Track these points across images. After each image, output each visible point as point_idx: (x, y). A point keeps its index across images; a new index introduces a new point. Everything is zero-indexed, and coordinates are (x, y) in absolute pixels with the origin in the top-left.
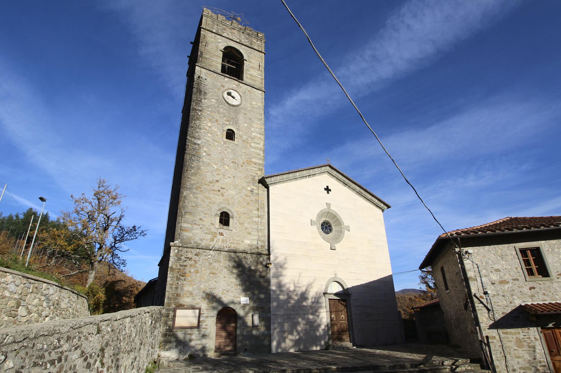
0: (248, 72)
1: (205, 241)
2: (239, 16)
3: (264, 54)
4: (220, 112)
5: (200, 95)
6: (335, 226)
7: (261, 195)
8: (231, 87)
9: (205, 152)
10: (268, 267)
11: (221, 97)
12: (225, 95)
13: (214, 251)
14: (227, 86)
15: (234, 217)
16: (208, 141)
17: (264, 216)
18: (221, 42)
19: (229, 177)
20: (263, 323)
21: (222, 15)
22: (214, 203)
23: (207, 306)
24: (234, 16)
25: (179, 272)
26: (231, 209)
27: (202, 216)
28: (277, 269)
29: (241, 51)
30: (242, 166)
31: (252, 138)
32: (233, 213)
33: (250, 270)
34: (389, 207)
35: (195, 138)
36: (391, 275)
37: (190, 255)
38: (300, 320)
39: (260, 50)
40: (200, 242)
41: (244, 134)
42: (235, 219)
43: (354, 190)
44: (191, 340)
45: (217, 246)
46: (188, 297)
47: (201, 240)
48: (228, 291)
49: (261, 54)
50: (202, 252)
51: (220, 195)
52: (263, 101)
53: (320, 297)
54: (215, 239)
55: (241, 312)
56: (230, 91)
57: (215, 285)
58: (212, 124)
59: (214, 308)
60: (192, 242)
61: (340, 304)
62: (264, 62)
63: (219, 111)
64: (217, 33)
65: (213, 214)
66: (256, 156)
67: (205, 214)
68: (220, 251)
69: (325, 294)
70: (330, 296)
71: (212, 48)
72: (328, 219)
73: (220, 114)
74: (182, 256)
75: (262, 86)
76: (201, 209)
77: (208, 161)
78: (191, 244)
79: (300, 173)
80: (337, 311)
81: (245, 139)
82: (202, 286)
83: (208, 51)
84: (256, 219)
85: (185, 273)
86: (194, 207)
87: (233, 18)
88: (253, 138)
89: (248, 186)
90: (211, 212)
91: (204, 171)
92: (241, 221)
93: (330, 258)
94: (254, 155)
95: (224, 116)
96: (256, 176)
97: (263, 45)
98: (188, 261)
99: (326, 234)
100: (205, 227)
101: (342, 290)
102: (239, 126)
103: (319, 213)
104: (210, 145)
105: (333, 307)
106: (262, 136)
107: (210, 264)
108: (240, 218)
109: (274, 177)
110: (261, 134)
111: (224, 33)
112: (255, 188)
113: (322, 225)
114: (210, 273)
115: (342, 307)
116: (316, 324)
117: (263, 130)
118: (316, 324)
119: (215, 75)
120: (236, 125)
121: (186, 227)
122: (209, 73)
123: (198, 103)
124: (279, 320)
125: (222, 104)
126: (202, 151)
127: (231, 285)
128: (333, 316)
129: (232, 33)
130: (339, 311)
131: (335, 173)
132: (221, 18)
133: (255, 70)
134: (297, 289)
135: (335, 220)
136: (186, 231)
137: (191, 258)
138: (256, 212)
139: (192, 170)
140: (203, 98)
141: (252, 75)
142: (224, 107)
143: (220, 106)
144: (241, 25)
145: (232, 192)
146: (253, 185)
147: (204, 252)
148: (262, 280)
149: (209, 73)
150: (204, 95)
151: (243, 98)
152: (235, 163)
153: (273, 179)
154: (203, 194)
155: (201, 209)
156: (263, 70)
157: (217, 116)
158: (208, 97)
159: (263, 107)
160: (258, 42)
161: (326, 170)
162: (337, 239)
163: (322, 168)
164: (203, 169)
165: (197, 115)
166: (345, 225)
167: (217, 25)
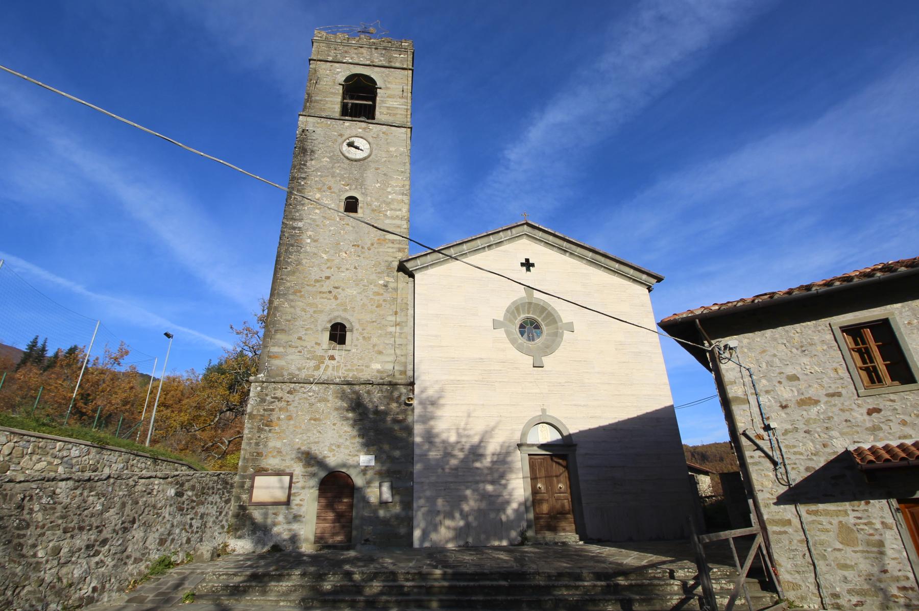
1: (305, 370)
5: (304, 156)
6: (546, 325)
7: (402, 289)
9: (310, 237)
10: (411, 405)
11: (337, 152)
12: (345, 148)
13: (318, 385)
14: (347, 133)
15: (354, 329)
16: (314, 220)
18: (341, 72)
19: (347, 269)
20: (397, 498)
22: (321, 312)
23: (303, 470)
24: (365, 28)
25: (262, 419)
26: (349, 317)
27: (302, 333)
28: (425, 408)
29: (372, 76)
30: (369, 249)
31: (388, 204)
32: (353, 323)
33: (377, 412)
34: (659, 280)
35: (295, 220)
36: (672, 406)
37: (279, 394)
38: (468, 492)
39: (405, 66)
40: (297, 372)
42: (355, 332)
43: (581, 258)
44: (274, 524)
45: (324, 377)
46: (274, 457)
47: (299, 369)
48: (339, 446)
49: (406, 72)
50: (298, 388)
51: (332, 298)
52: (409, 141)
53: (508, 454)
54: (323, 366)
55: (359, 481)
56: (352, 139)
57: (319, 437)
58: (321, 195)
59: (313, 475)
60: (285, 373)
61: (554, 464)
63: (334, 172)
65: (320, 328)
67: (306, 330)
68: (328, 384)
70: (531, 448)
72: (532, 314)
73: (336, 177)
74: (267, 395)
75: (408, 121)
76: (301, 323)
77: (314, 250)
78: (283, 376)
79: (469, 244)
80: (549, 477)
82: (297, 440)
84: (392, 329)
85: (271, 421)
86: (289, 321)
88: (390, 203)
89: (380, 278)
90: (316, 326)
91: (307, 265)
92: (366, 335)
93: (531, 382)
95: (343, 178)
96: (393, 261)
101: (559, 437)
103: (510, 307)
104: (317, 226)
107: (311, 405)
108: (363, 330)
109: (421, 258)
110: (403, 194)
111: (346, 57)
112: (391, 280)
113: (522, 326)
114: (310, 419)
115: (557, 469)
116: (500, 500)
117: (407, 187)
118: (500, 500)
120: (361, 188)
122: (319, 121)
123: (301, 168)
124: (428, 493)
126: (304, 236)
127: (345, 437)
128: (539, 485)
129: (359, 53)
130: (554, 476)
133: (395, 99)
134: (464, 440)
135: (544, 314)
138: (393, 318)
141: (389, 107)
142: (342, 165)
143: (336, 165)
145: (352, 291)
146: (388, 276)
147: (302, 387)
148: (396, 427)
149: (319, 121)
150: (311, 155)
152: (358, 246)
153: (419, 262)
154: (304, 301)
155: (301, 323)
157: (330, 181)
158: (316, 156)
159: (409, 152)
160: (401, 56)
161: (523, 232)
162: (547, 347)
164: (306, 263)
165: (299, 185)
167: (336, 49)
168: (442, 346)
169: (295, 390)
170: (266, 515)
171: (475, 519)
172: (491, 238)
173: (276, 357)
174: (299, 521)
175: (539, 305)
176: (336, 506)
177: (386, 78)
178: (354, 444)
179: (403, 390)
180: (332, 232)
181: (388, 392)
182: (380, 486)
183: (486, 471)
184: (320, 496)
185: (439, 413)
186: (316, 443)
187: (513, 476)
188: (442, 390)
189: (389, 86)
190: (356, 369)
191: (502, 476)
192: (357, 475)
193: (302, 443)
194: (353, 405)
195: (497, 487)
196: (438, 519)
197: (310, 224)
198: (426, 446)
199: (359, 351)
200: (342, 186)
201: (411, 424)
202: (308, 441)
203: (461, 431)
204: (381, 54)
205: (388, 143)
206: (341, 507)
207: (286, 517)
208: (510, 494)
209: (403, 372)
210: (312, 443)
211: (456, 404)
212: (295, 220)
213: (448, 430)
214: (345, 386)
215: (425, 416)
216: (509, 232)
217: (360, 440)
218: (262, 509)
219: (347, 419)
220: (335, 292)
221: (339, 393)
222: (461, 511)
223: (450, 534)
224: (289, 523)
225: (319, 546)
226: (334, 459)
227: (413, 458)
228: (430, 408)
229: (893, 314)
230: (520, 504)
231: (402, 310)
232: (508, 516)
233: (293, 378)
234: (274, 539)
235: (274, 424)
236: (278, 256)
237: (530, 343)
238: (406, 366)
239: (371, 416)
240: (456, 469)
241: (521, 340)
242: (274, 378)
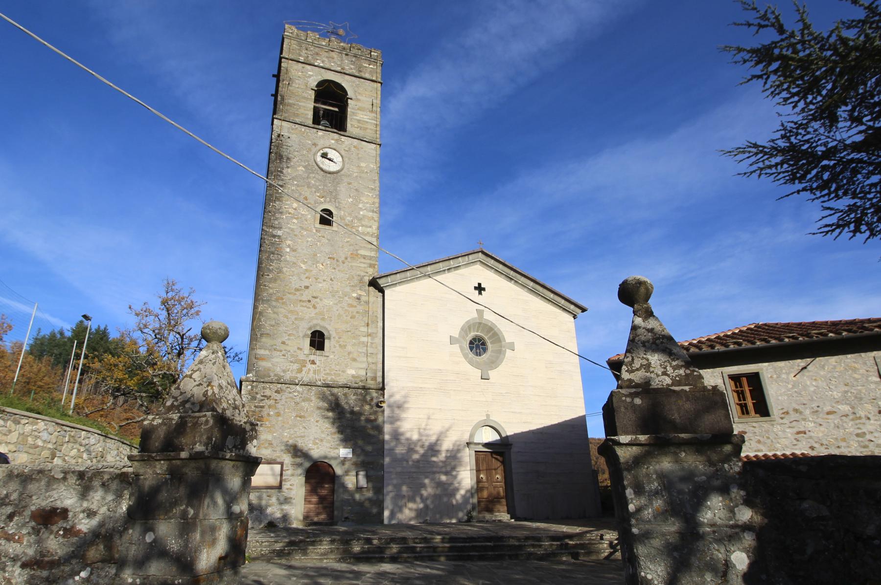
0: (355, 117)
3: (380, 84)
4: (311, 185)
5: (280, 163)
7: (373, 303)
8: (327, 144)
9: (289, 246)
10: (382, 407)
11: (312, 163)
12: (319, 159)
13: (302, 386)
14: (321, 143)
15: (332, 337)
16: (292, 230)
17: (376, 333)
18: (312, 75)
19: (324, 281)
20: (370, 485)
21: (313, 30)
22: (302, 319)
23: (292, 460)
24: (334, 28)
26: (327, 326)
28: (393, 411)
29: (343, 85)
30: (343, 263)
31: (360, 220)
33: (352, 412)
35: (274, 227)
37: (268, 393)
39: (374, 78)
40: (282, 374)
41: (347, 214)
42: (332, 340)
45: (306, 380)
47: (284, 371)
48: (322, 440)
49: (375, 85)
50: (285, 388)
52: (378, 159)
55: (339, 471)
56: (326, 150)
58: (298, 205)
60: (272, 374)
62: (380, 96)
64: (305, 62)
65: (301, 335)
66: (365, 246)
67: (288, 335)
69: (468, 444)
71: (298, 88)
74: (257, 393)
75: (377, 138)
76: (284, 328)
77: (293, 259)
79: (433, 266)
81: (349, 221)
82: (286, 434)
83: (293, 93)
84: (365, 339)
86: (273, 326)
87: (332, 33)
88: (361, 219)
89: (353, 291)
90: (298, 332)
91: (287, 274)
94: (362, 245)
95: (318, 190)
97: (379, 70)
98: (266, 401)
100: (289, 353)
102: (339, 203)
104: (296, 235)
105: (482, 463)
106: (376, 214)
107: (297, 403)
108: (340, 338)
109: (392, 276)
110: (373, 211)
111: (317, 59)
112: (363, 293)
114: (297, 416)
117: (377, 205)
119: (303, 128)
120: (335, 201)
121: (263, 355)
122: (293, 127)
123: (278, 175)
124: (395, 482)
125: (313, 173)
126: (284, 245)
129: (330, 57)
132: (312, 36)
136: (263, 359)
137: (270, 397)
138: (364, 329)
139: (270, 275)
140: (285, 166)
142: (317, 176)
143: (311, 175)
144: (344, 42)
145: (329, 302)
146: (360, 289)
147: (288, 388)
149: (293, 127)
150: (287, 162)
151: (346, 159)
153: (389, 279)
155: (284, 328)
156: (379, 110)
157: (306, 192)
158: (292, 164)
159: (378, 169)
160: (371, 66)
164: (286, 271)
165: (276, 193)
167: (307, 49)
172: (451, 262)
176: (319, 491)
177: (356, 89)
179: (374, 394)
180: (309, 243)
182: (357, 475)
185: (404, 415)
186: (302, 437)
189: (358, 97)
192: (338, 465)
201: (381, 424)
202: (295, 435)
203: (422, 430)
206: (324, 492)
209: (374, 378)
210: (299, 437)
211: (419, 408)
212: (274, 227)
213: (412, 430)
214: (325, 389)
215: (392, 417)
217: (340, 436)
219: (327, 418)
221: (320, 394)
222: (422, 496)
226: (319, 450)
227: (383, 452)
228: (397, 411)
229: (762, 369)
231: (372, 322)
233: (281, 379)
238: (376, 374)
240: (418, 461)
242: (264, 379)
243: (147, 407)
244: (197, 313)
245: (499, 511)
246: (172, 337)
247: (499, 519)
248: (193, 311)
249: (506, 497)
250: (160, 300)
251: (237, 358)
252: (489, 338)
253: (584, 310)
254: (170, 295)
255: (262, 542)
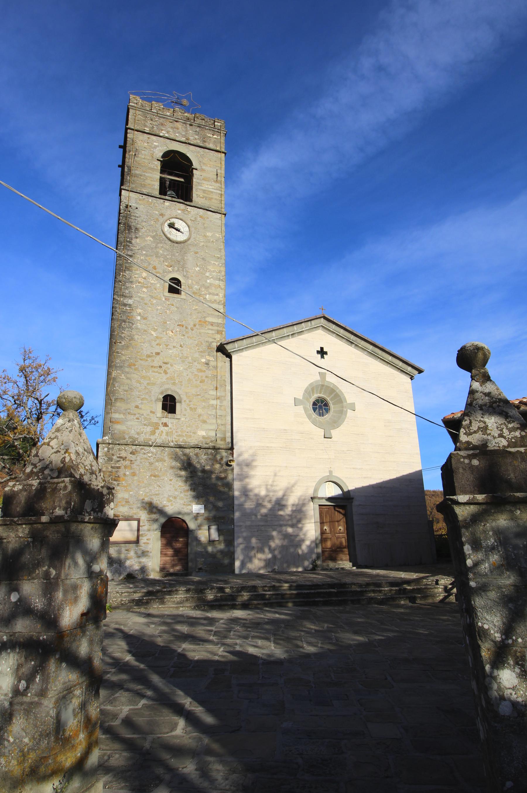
0: (200, 187)
1: (143, 435)
2: (185, 97)
3: (224, 155)
4: (160, 255)
5: (129, 233)
6: (333, 404)
7: (221, 368)
8: (174, 214)
9: (139, 314)
10: (231, 465)
12: (166, 228)
14: (168, 213)
15: (183, 401)
16: (142, 299)
17: (225, 396)
18: (158, 146)
19: (174, 347)
20: (222, 538)
21: (157, 101)
22: (154, 384)
23: (148, 516)
24: (178, 98)
25: (111, 475)
26: (178, 390)
27: (138, 402)
28: (241, 469)
29: (188, 155)
30: (192, 330)
31: (207, 288)
32: (181, 396)
33: (204, 471)
35: (125, 296)
37: (123, 454)
38: (274, 533)
39: (218, 149)
40: (136, 436)
41: (194, 283)
42: (183, 403)
43: (363, 349)
44: (127, 559)
45: (159, 441)
46: (123, 506)
47: (138, 434)
48: (175, 498)
50: (139, 449)
51: (162, 372)
52: (223, 229)
53: (304, 505)
54: (157, 432)
55: (192, 525)
56: (173, 220)
57: (159, 490)
59: (156, 520)
60: (127, 437)
61: (336, 513)
62: (223, 167)
63: (158, 252)
64: (151, 132)
65: (153, 399)
66: (212, 313)
67: (142, 400)
68: (163, 447)
71: (144, 159)
72: (323, 394)
73: (159, 257)
74: (113, 455)
76: (137, 393)
77: (144, 327)
78: (125, 439)
79: (277, 332)
81: (197, 290)
82: (141, 492)
83: (139, 164)
84: (214, 402)
85: (119, 477)
86: (127, 391)
87: (176, 103)
88: (208, 287)
89: (202, 357)
91: (139, 341)
92: (192, 406)
93: (322, 450)
94: (210, 313)
95: (166, 260)
96: (213, 342)
97: (223, 139)
98: (122, 462)
99: (320, 416)
100: (142, 417)
102: (187, 272)
103: (307, 388)
104: (146, 304)
106: (222, 282)
107: (151, 464)
108: (190, 401)
109: (238, 342)
110: (219, 280)
111: (162, 130)
112: (212, 359)
113: (314, 404)
114: (151, 476)
116: (298, 539)
117: (223, 273)
118: (298, 539)
119: (150, 199)
121: (117, 418)
123: (127, 245)
124: (245, 534)
125: (161, 243)
127: (180, 490)
131: (333, 327)
133: (210, 183)
134: (271, 494)
135: (333, 395)
136: (118, 423)
137: (126, 458)
138: (213, 393)
139: (122, 342)
140: (134, 236)
141: (205, 190)
142: (165, 246)
143: (159, 245)
144: (188, 112)
145: (179, 367)
146: (209, 355)
148: (220, 483)
149: (141, 197)
150: (135, 232)
151: (192, 229)
152: (183, 326)
153: (236, 344)
154: (138, 374)
155: (137, 393)
156: (223, 179)
157: (154, 261)
158: (140, 234)
159: (224, 238)
160: (214, 136)
161: (320, 324)
162: (335, 422)
163: (313, 322)
164: (138, 338)
166: (349, 401)
167: (152, 120)
168: (255, 419)
169: (136, 451)
170: (119, 552)
171: (280, 552)
172: (295, 327)
173: (117, 422)
174: (147, 555)
175: (329, 387)
176: (174, 544)
177: (201, 159)
178: (187, 496)
179: (224, 453)
180: (158, 311)
181: (212, 455)
182: (209, 529)
183: (287, 517)
184: (162, 536)
185: (252, 473)
186: (157, 495)
187: (308, 521)
188: (254, 455)
189: (204, 167)
190: (186, 435)
191: (299, 521)
192: (191, 520)
193: (145, 495)
194: (185, 465)
195: (296, 529)
196: (252, 553)
197: (139, 302)
198: (243, 499)
199: (187, 420)
200: (166, 267)
201: (231, 481)
202: (151, 493)
203: (269, 487)
204: (196, 131)
205: (205, 228)
206: (178, 545)
207: (136, 553)
208: (305, 535)
209: (224, 439)
210: (154, 495)
211: (266, 466)
212: (125, 296)
213: (260, 486)
214: (178, 449)
215: (241, 475)
216: (309, 323)
217: (193, 493)
218: (117, 546)
219: (181, 476)
220: (165, 367)
221: (173, 455)
222: (270, 547)
223: (262, 564)
224: (139, 557)
225: (164, 574)
226: (172, 507)
227: (234, 507)
228: (246, 469)
230: (312, 542)
231: (221, 386)
232: (303, 551)
233: (135, 441)
234: (128, 570)
235: (121, 479)
236: (112, 331)
237: (319, 417)
238: (225, 434)
239: (200, 474)
240: (266, 515)
241: (314, 415)
242: (119, 441)
243: (9, 469)
244: (54, 380)
245: (342, 560)
246: (30, 403)
247: (342, 567)
248: (49, 378)
249: (348, 547)
250: (18, 368)
251: (93, 421)
252: (331, 400)
253: (420, 371)
254: (27, 362)
255: (122, 593)
